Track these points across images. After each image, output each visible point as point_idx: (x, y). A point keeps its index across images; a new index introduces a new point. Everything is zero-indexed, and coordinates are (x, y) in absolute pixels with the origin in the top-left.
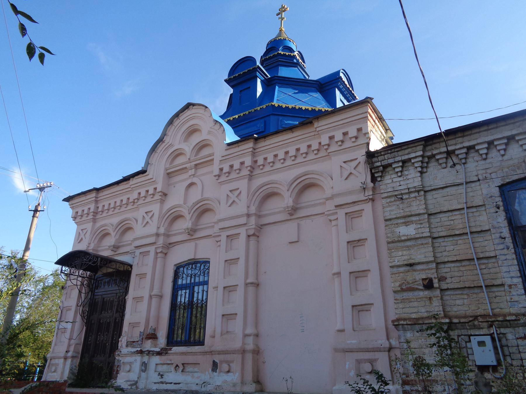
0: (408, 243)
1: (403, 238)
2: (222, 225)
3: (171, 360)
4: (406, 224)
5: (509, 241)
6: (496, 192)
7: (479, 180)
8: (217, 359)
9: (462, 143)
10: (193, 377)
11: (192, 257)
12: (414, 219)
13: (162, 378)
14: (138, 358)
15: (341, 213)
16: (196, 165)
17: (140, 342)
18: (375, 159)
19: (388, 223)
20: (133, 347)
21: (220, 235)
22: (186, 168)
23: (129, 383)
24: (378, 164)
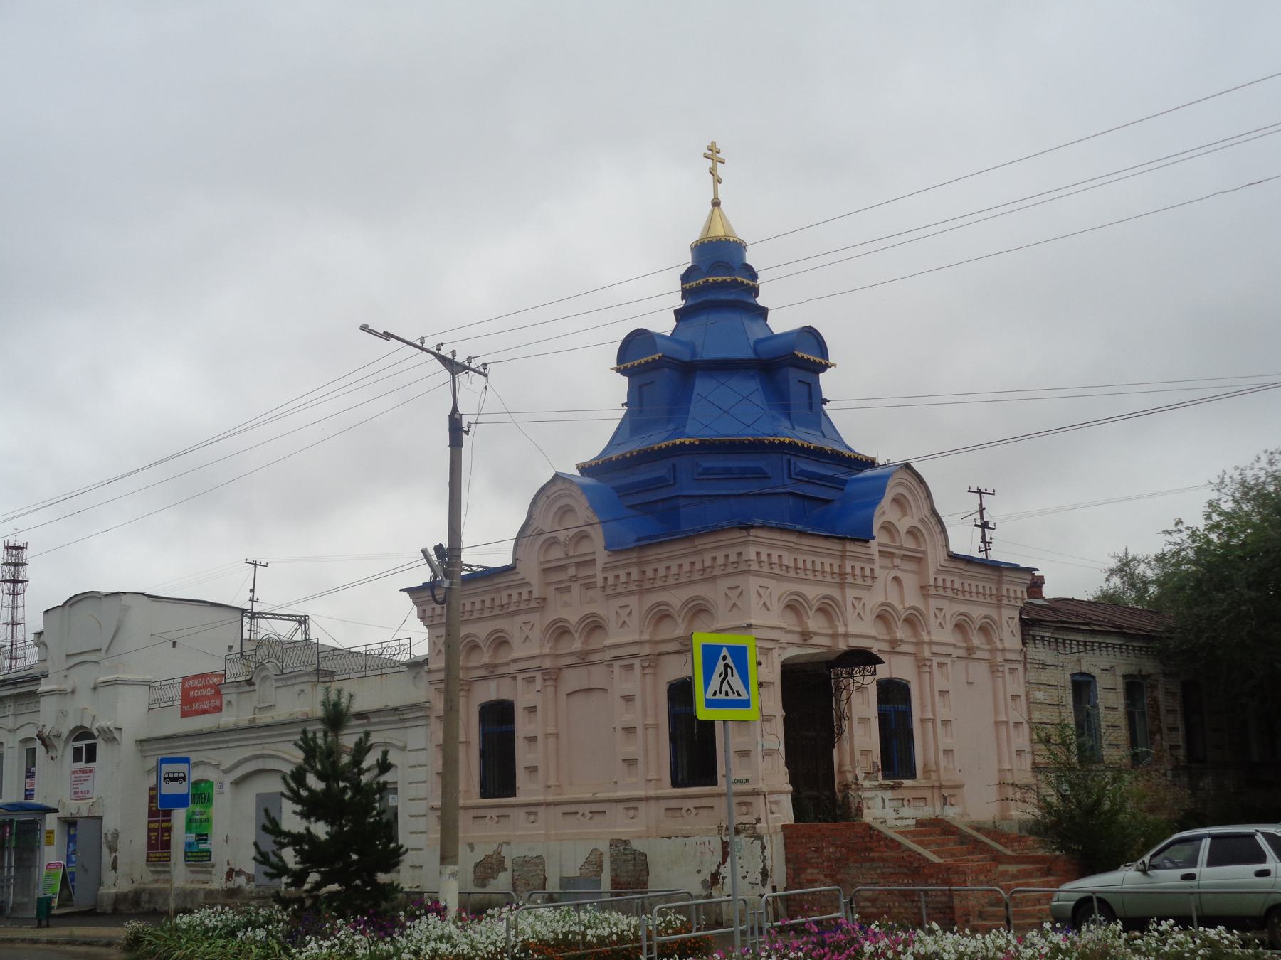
0: (1039, 706)
1: (1038, 701)
2: (936, 649)
3: (902, 795)
4: (1039, 690)
5: (1073, 714)
6: (1069, 678)
7: (1062, 666)
8: (945, 792)
9: (1063, 635)
10: (923, 810)
11: (888, 676)
12: (1041, 686)
13: (898, 814)
14: (880, 793)
15: (1008, 666)
16: (904, 555)
17: (875, 774)
18: (1031, 628)
19: (1030, 686)
20: (870, 780)
21: (931, 660)
22: (892, 554)
23: (879, 821)
24: (1031, 633)
